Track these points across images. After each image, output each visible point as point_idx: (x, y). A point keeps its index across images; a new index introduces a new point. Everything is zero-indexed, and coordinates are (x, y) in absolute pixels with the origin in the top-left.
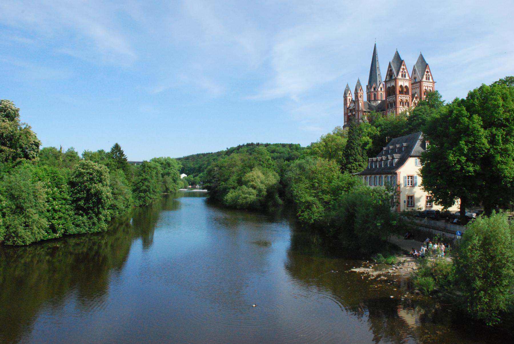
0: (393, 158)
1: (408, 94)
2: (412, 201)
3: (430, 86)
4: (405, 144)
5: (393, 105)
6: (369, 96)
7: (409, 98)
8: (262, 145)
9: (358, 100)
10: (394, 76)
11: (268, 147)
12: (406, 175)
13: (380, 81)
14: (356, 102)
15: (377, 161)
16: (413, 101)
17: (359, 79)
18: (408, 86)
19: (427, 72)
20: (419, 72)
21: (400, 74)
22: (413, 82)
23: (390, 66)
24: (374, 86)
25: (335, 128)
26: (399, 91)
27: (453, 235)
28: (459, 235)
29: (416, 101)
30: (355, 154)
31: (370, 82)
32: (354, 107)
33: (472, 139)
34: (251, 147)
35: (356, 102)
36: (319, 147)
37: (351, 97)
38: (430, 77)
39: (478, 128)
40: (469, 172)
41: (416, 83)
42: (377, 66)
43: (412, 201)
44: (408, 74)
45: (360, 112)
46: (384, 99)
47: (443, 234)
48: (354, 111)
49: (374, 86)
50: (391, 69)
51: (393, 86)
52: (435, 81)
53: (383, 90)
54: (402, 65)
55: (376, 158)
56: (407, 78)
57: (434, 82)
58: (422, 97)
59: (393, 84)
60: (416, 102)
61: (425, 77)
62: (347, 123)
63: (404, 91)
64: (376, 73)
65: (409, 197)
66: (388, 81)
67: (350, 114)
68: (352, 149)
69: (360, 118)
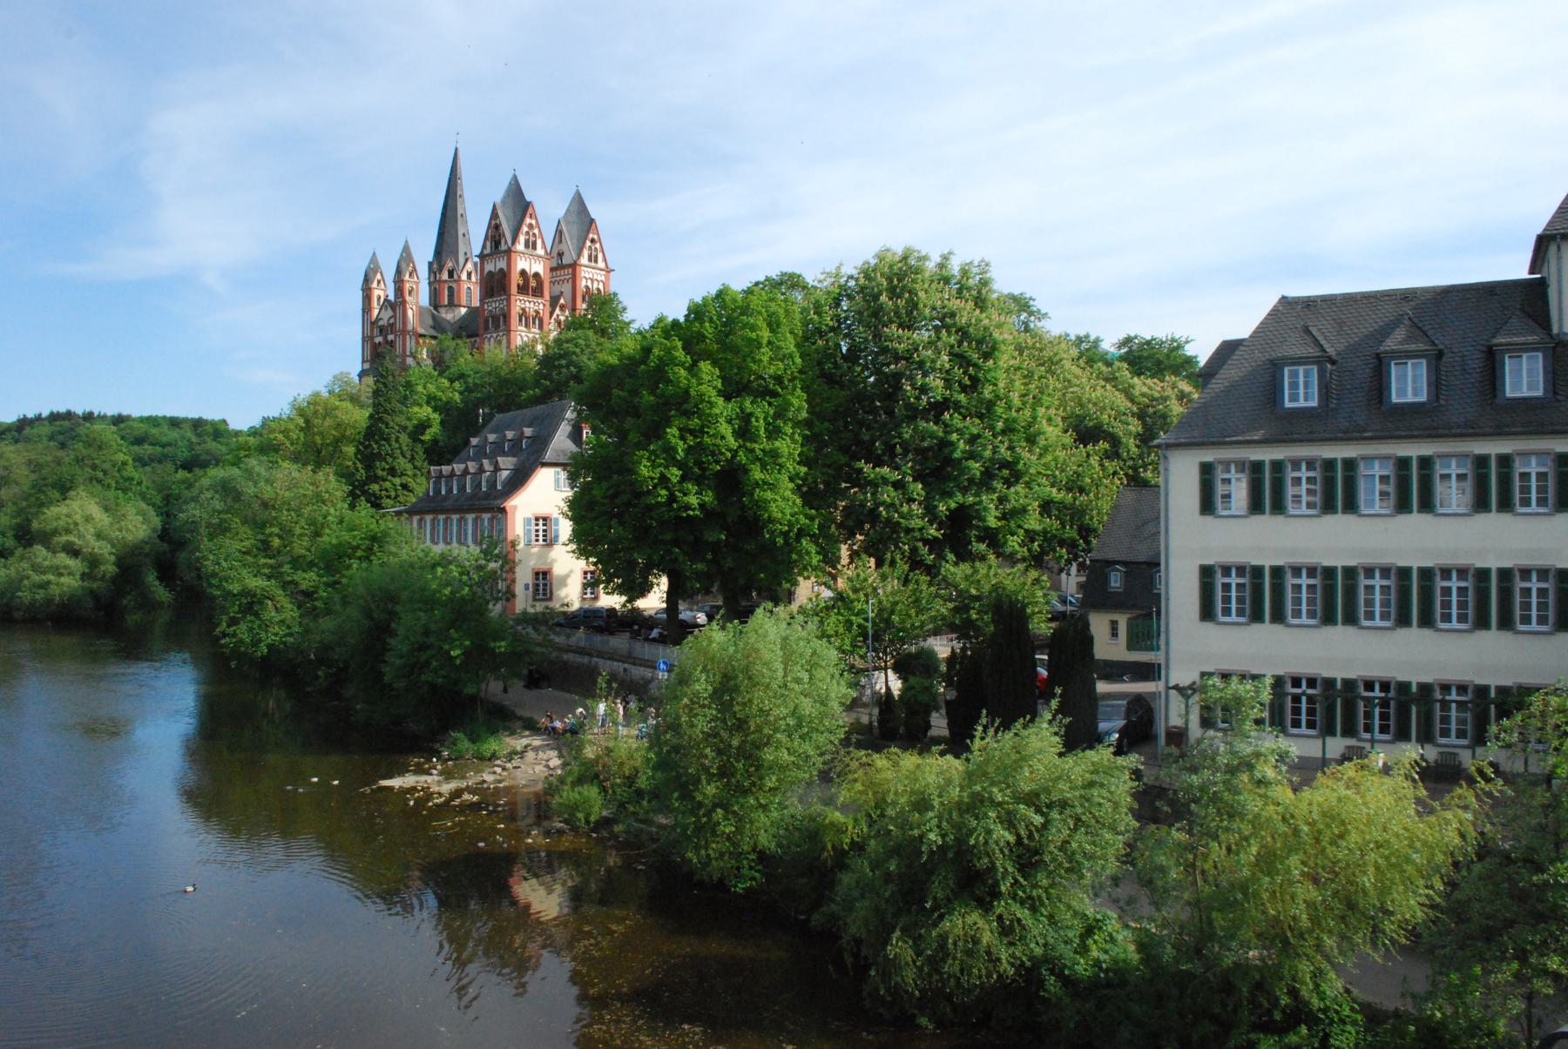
0: (497, 469)
1: (542, 296)
2: (545, 585)
3: (599, 278)
4: (528, 431)
5: (501, 322)
6: (435, 293)
7: (544, 305)
8: (102, 418)
9: (404, 302)
10: (506, 242)
11: (122, 425)
12: (530, 515)
13: (466, 254)
14: (397, 304)
15: (452, 474)
16: (555, 316)
17: (406, 242)
18: (542, 274)
21: (522, 238)
22: (555, 265)
23: (494, 215)
24: (450, 265)
25: (335, 377)
26: (518, 285)
27: (649, 670)
28: (663, 671)
30: (391, 456)
31: (438, 253)
32: (392, 321)
33: (695, 422)
34: (66, 423)
35: (397, 304)
36: (285, 432)
37: (383, 290)
39: (710, 397)
40: (688, 507)
41: (564, 267)
42: (460, 211)
43: (545, 585)
44: (543, 242)
45: (408, 337)
46: (476, 303)
47: (625, 670)
48: (392, 333)
49: (450, 265)
51: (501, 270)
52: (611, 266)
53: (473, 279)
54: (528, 215)
55: (449, 468)
57: (608, 271)
59: (502, 264)
60: (562, 318)
61: (586, 253)
62: (371, 366)
63: (532, 286)
65: (537, 574)
66: (487, 255)
67: (379, 339)
68: (385, 440)
69: (408, 353)
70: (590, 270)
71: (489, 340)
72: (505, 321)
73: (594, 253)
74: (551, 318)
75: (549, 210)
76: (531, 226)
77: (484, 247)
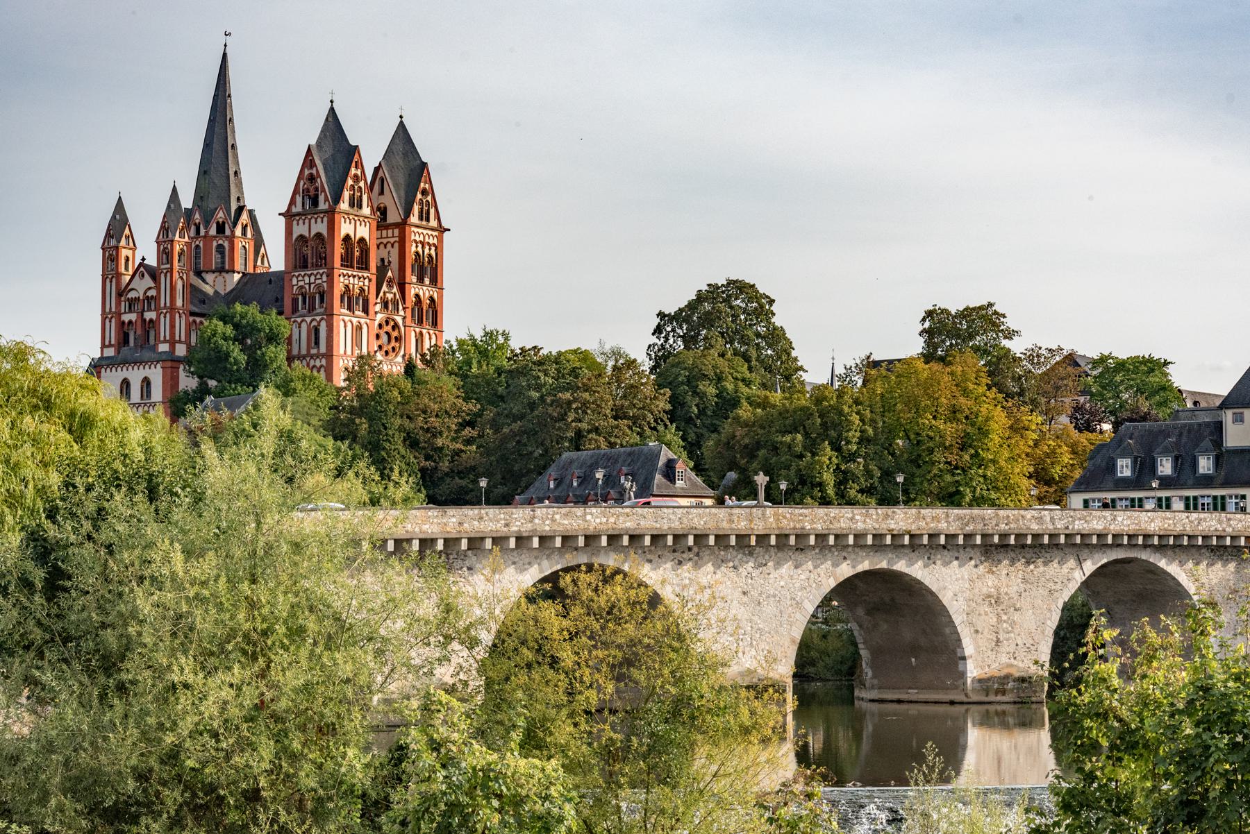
1: (367, 268)
3: (431, 241)
5: (317, 302)
7: (370, 280)
17: (174, 190)
18: (367, 239)
19: (424, 192)
20: (397, 191)
21: (346, 194)
23: (309, 161)
24: (220, 215)
29: (388, 295)
31: (199, 197)
32: (152, 293)
38: (432, 211)
45: (177, 315)
48: (150, 310)
50: (314, 171)
51: (319, 235)
53: (249, 235)
54: (354, 164)
56: (366, 211)
57: (442, 230)
58: (407, 280)
59: (321, 227)
61: (416, 208)
63: (356, 254)
66: (298, 214)
67: (126, 318)
69: (177, 338)
70: (420, 230)
72: (322, 301)
74: (377, 298)
75: (372, 155)
76: (356, 175)
77: (292, 202)
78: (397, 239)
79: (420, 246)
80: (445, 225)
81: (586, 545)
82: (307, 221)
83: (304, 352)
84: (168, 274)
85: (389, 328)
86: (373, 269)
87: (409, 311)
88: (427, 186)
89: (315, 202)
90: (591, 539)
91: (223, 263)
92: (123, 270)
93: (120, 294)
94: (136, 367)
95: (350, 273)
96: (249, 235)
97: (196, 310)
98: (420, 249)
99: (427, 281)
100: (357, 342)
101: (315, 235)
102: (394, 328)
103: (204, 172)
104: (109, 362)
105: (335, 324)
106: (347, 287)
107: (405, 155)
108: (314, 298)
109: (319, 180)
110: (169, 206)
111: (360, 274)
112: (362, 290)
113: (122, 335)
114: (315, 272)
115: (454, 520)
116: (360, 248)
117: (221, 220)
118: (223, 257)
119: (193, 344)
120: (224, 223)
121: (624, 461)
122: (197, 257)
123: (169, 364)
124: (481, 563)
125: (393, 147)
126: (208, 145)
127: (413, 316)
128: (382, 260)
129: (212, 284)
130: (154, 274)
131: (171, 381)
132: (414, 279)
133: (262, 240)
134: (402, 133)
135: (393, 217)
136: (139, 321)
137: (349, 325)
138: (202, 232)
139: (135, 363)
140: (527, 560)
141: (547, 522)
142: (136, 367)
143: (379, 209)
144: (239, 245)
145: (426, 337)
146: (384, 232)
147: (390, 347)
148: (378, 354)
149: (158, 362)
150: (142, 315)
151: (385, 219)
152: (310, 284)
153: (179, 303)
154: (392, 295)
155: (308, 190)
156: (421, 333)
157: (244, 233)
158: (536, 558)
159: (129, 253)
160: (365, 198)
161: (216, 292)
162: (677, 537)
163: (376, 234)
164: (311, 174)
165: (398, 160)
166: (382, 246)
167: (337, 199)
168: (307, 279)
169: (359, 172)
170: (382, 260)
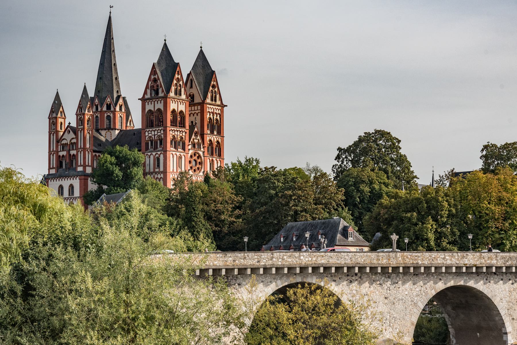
1: (184, 127)
3: (217, 112)
7: (186, 133)
16: (192, 140)
17: (85, 87)
19: (213, 86)
20: (199, 85)
21: (173, 88)
23: (153, 71)
24: (109, 100)
29: (195, 140)
31: (98, 91)
32: (74, 141)
38: (218, 96)
45: (87, 152)
48: (73, 149)
50: (156, 77)
51: (159, 110)
53: (123, 110)
54: (177, 72)
56: (183, 97)
57: (223, 106)
58: (205, 132)
59: (160, 106)
60: (196, 141)
61: (209, 95)
62: (57, 171)
64: (112, 77)
66: (148, 99)
67: (61, 154)
69: (87, 164)
70: (212, 106)
71: (150, 157)
72: (161, 144)
73: (214, 95)
74: (189, 142)
76: (178, 78)
77: (145, 93)
78: (199, 111)
79: (212, 114)
80: (224, 103)
81: (301, 272)
82: (153, 102)
83: (152, 170)
84: (82, 131)
85: (196, 158)
86: (187, 127)
87: (206, 149)
88: (215, 83)
89: (157, 93)
90: (303, 269)
91: (110, 125)
92: (59, 129)
93: (58, 142)
94: (66, 179)
95: (175, 129)
96: (123, 110)
97: (96, 149)
98: (211, 116)
99: (215, 133)
100: (179, 165)
101: (157, 110)
102: (198, 157)
103: (100, 78)
104: (52, 176)
105: (168, 156)
106: (174, 136)
107: (203, 67)
108: (157, 142)
109: (159, 81)
110: (82, 96)
111: (181, 130)
112: (182, 138)
113: (59, 163)
114: (157, 129)
115: (231, 259)
116: (181, 116)
117: (109, 103)
118: (110, 122)
119: (95, 167)
120: (110, 104)
121: (321, 227)
122: (97, 122)
123: (83, 177)
124: (245, 281)
125: (197, 63)
126: (102, 64)
127: (208, 151)
128: (192, 122)
129: (104, 135)
130: (75, 131)
131: (84, 186)
132: (209, 132)
133: (130, 113)
134: (202, 57)
135: (197, 100)
136: (68, 156)
137: (175, 156)
138: (99, 109)
139: (66, 177)
140: (269, 280)
141: (280, 260)
142: (66, 179)
143: (190, 95)
144: (118, 115)
145: (216, 162)
146: (193, 108)
147: (196, 168)
148: (190, 171)
149: (77, 176)
150: (69, 152)
151: (193, 101)
152: (155, 135)
153: (88, 146)
154: (197, 140)
155: (153, 86)
156: (213, 160)
157: (121, 109)
158: (274, 279)
159: (62, 120)
160: (183, 90)
161: (106, 140)
162: (349, 268)
163: (188, 109)
164: (155, 78)
165: (200, 70)
166: (192, 115)
167: (168, 91)
168: (153, 133)
169: (179, 77)
170: (192, 122)
